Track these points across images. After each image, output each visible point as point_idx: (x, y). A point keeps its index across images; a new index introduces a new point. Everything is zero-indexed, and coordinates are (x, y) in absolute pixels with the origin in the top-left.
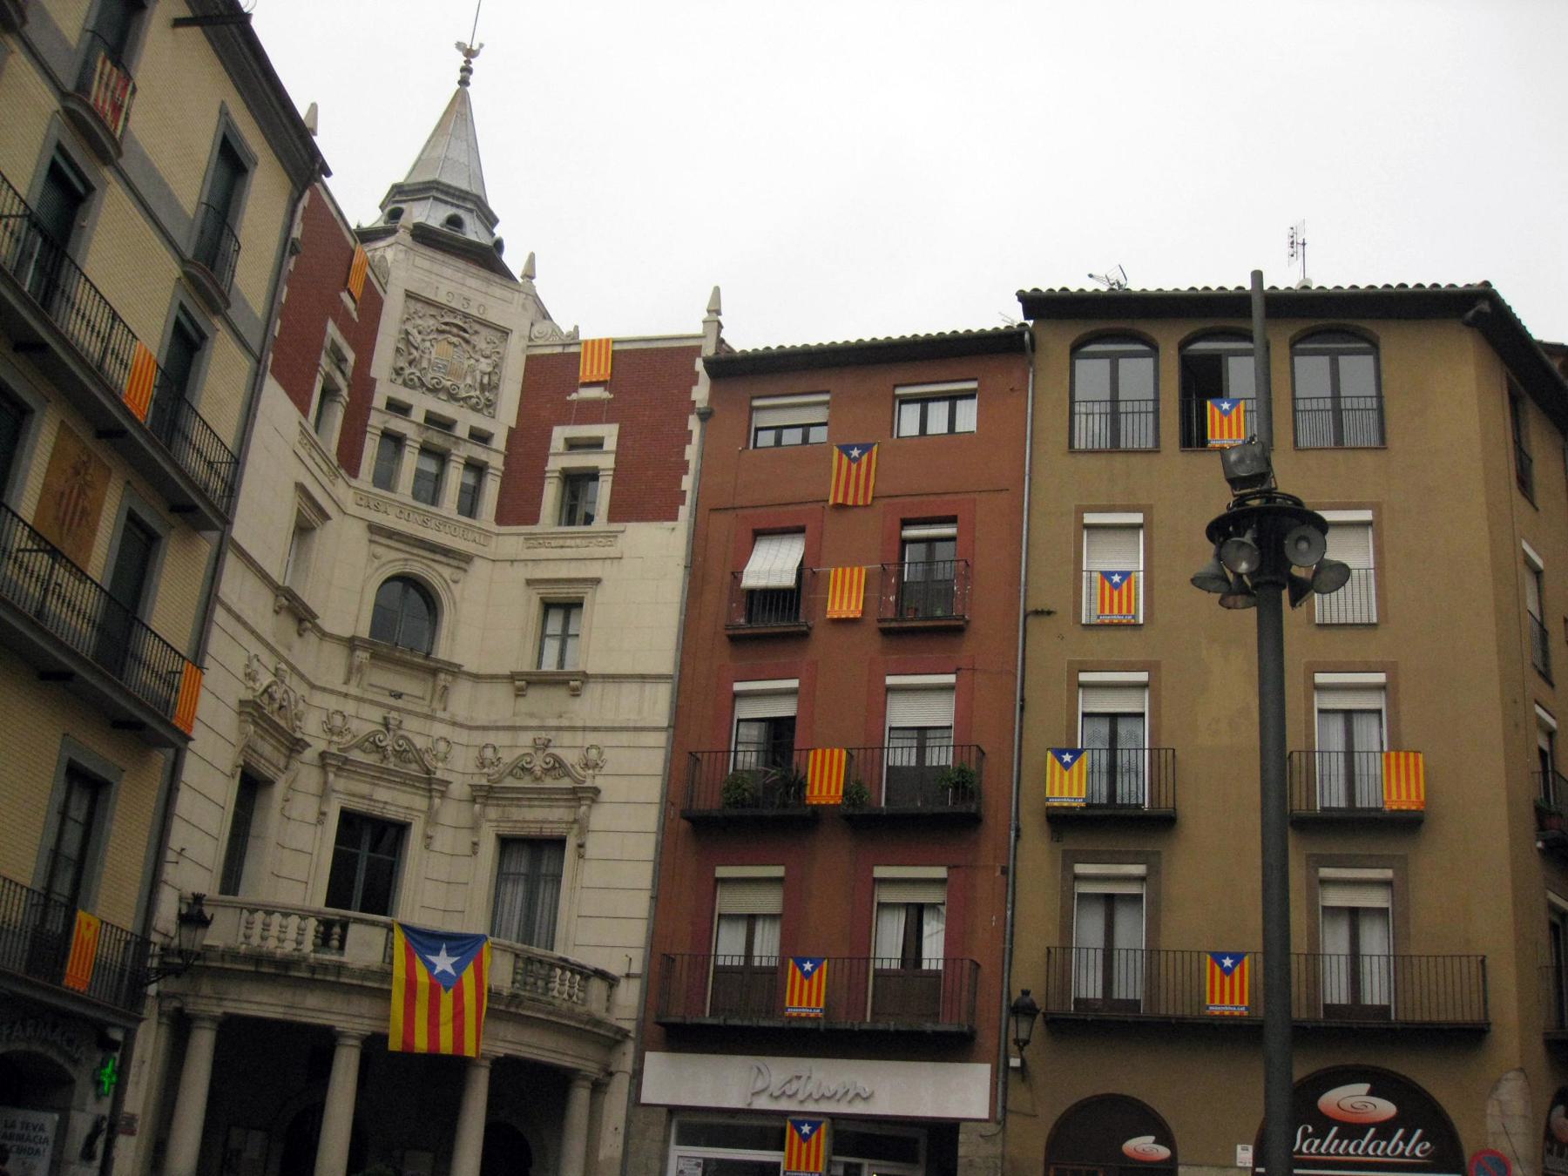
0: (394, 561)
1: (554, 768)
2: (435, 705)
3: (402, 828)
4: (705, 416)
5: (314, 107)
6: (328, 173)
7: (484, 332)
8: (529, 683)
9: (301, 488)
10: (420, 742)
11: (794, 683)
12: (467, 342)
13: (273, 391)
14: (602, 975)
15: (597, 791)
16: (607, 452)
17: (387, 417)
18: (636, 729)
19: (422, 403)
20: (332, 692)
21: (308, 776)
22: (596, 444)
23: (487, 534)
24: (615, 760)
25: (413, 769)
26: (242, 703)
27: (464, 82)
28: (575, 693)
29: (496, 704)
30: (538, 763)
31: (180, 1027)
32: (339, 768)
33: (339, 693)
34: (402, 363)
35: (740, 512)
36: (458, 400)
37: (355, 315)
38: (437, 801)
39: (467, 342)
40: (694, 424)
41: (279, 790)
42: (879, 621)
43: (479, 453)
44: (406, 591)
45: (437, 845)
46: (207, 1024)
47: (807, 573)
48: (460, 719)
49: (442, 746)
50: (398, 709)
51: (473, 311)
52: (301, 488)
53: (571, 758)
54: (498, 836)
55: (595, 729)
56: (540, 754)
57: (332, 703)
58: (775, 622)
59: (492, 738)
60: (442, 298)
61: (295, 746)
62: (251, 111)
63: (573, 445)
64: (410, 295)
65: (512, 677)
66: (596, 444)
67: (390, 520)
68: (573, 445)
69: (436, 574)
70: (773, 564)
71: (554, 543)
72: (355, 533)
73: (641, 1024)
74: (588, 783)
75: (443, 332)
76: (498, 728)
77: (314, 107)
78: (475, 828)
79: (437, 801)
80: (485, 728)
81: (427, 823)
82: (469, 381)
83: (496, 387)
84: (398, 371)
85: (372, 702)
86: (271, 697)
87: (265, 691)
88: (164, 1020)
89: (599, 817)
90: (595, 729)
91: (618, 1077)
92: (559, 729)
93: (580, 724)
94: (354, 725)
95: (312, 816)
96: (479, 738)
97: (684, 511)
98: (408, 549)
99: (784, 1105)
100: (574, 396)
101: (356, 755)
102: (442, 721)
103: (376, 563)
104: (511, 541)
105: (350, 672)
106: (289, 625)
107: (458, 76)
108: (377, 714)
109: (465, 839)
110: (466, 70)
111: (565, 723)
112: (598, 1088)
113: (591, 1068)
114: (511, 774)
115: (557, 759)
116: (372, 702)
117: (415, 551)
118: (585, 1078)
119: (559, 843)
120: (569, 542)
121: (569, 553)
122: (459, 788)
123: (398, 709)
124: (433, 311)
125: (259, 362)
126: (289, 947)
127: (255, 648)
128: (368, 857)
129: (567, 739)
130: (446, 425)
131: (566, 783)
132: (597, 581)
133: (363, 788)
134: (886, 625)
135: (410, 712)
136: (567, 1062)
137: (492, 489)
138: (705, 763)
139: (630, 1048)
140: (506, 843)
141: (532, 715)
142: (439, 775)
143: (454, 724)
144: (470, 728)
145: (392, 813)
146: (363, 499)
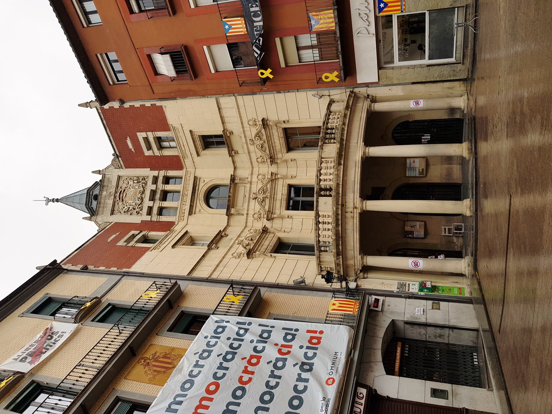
0: (200, 203)
1: (259, 136)
2: (246, 182)
4: (122, 102)
5: (37, 268)
6: (55, 261)
7: (120, 185)
8: (233, 150)
9: (173, 247)
10: (260, 185)
11: (205, 48)
12: (124, 190)
13: (136, 268)
14: (330, 105)
15: (263, 120)
16: (147, 135)
17: (153, 215)
18: (238, 108)
19: (147, 203)
20: (247, 219)
21: (277, 224)
22: (146, 140)
23: (187, 172)
24: (252, 115)
25: (269, 186)
26: (248, 257)
27: (57, 200)
28: (231, 133)
29: (242, 159)
30: (259, 142)
31: (367, 269)
32: (272, 213)
33: (247, 217)
34: (135, 212)
35: (151, 83)
36: (144, 190)
38: (279, 176)
39: (124, 190)
40: (127, 105)
41: (281, 235)
42: (170, 16)
44: (212, 198)
45: (294, 174)
46: (365, 261)
47: (163, 50)
48: (250, 173)
49: (260, 177)
50: (250, 194)
52: (173, 247)
53: (254, 131)
54: (287, 153)
55: (242, 123)
56: (255, 142)
57: (250, 219)
58: (186, 61)
59: (254, 160)
61: (265, 231)
62: (26, 301)
63: (149, 148)
64: (112, 213)
65: (231, 155)
66: (146, 140)
67: (187, 208)
68: (149, 148)
69: (202, 189)
70: (164, 65)
71: (183, 149)
73: (347, 87)
74: (261, 123)
75: (123, 200)
76: (250, 159)
77: (37, 268)
78: (286, 161)
79: (279, 176)
80: (252, 163)
81: (287, 179)
82: (137, 187)
83: (138, 177)
84: (138, 213)
85: (248, 206)
86: (247, 245)
87: (245, 248)
88: (366, 275)
89: (272, 117)
90: (242, 123)
91: (369, 93)
92: (245, 137)
93: (242, 129)
95: (290, 220)
96: (255, 164)
97: (158, 103)
98: (195, 200)
99: (372, 19)
100: (133, 150)
101: (267, 208)
102: (251, 178)
103: (202, 210)
104: (188, 163)
105: (239, 214)
106: (224, 240)
108: (252, 202)
109: (290, 164)
110: (53, 200)
111: (243, 135)
112: (374, 100)
113: (367, 103)
114: (265, 151)
115: (256, 136)
116: (248, 206)
117: (196, 197)
118: (370, 106)
119: (285, 130)
120: (182, 144)
121: (185, 143)
122: (273, 169)
123: (250, 194)
124: (116, 204)
125: (124, 275)
126: (330, 233)
127: (229, 255)
128: (301, 198)
129: (248, 133)
130: (153, 193)
131: (263, 131)
132: (191, 131)
133: (278, 203)
134: (171, 12)
135: (250, 190)
136: (364, 115)
137: (171, 173)
138: (244, 79)
139: (356, 90)
140: (289, 149)
141: (243, 147)
142: (270, 177)
143: (252, 174)
144: (253, 168)
146: (181, 219)
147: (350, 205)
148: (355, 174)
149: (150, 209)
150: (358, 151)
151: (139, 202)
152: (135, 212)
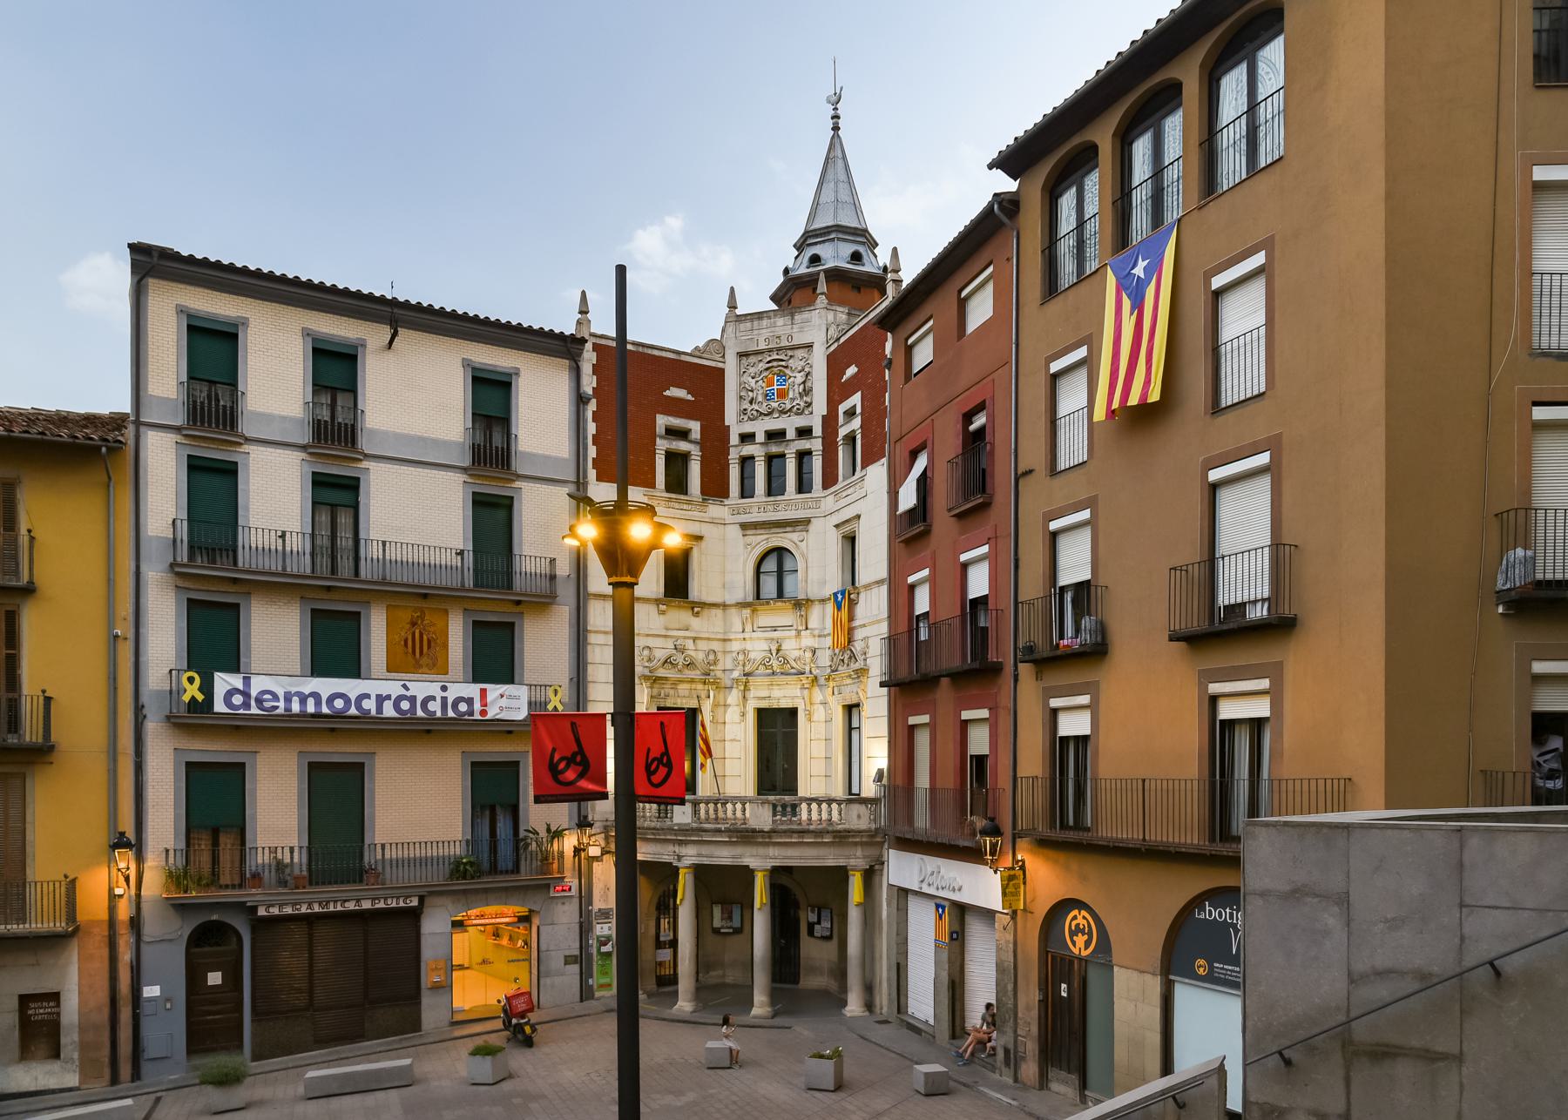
3: (793, 712)
19: (760, 428)
21: (734, 697)
23: (818, 500)
27: (836, 128)
34: (746, 405)
37: (690, 397)
42: (949, 510)
43: (804, 444)
51: (784, 343)
60: (762, 346)
72: (735, 531)
94: (752, 656)
95: (737, 718)
107: (830, 124)
121: (849, 500)
132: (858, 517)
145: (785, 704)
146: (736, 511)
147: (684, 850)
148: (724, 856)
149: (747, 438)
150: (759, 860)
151: (764, 409)
152: (746, 405)
